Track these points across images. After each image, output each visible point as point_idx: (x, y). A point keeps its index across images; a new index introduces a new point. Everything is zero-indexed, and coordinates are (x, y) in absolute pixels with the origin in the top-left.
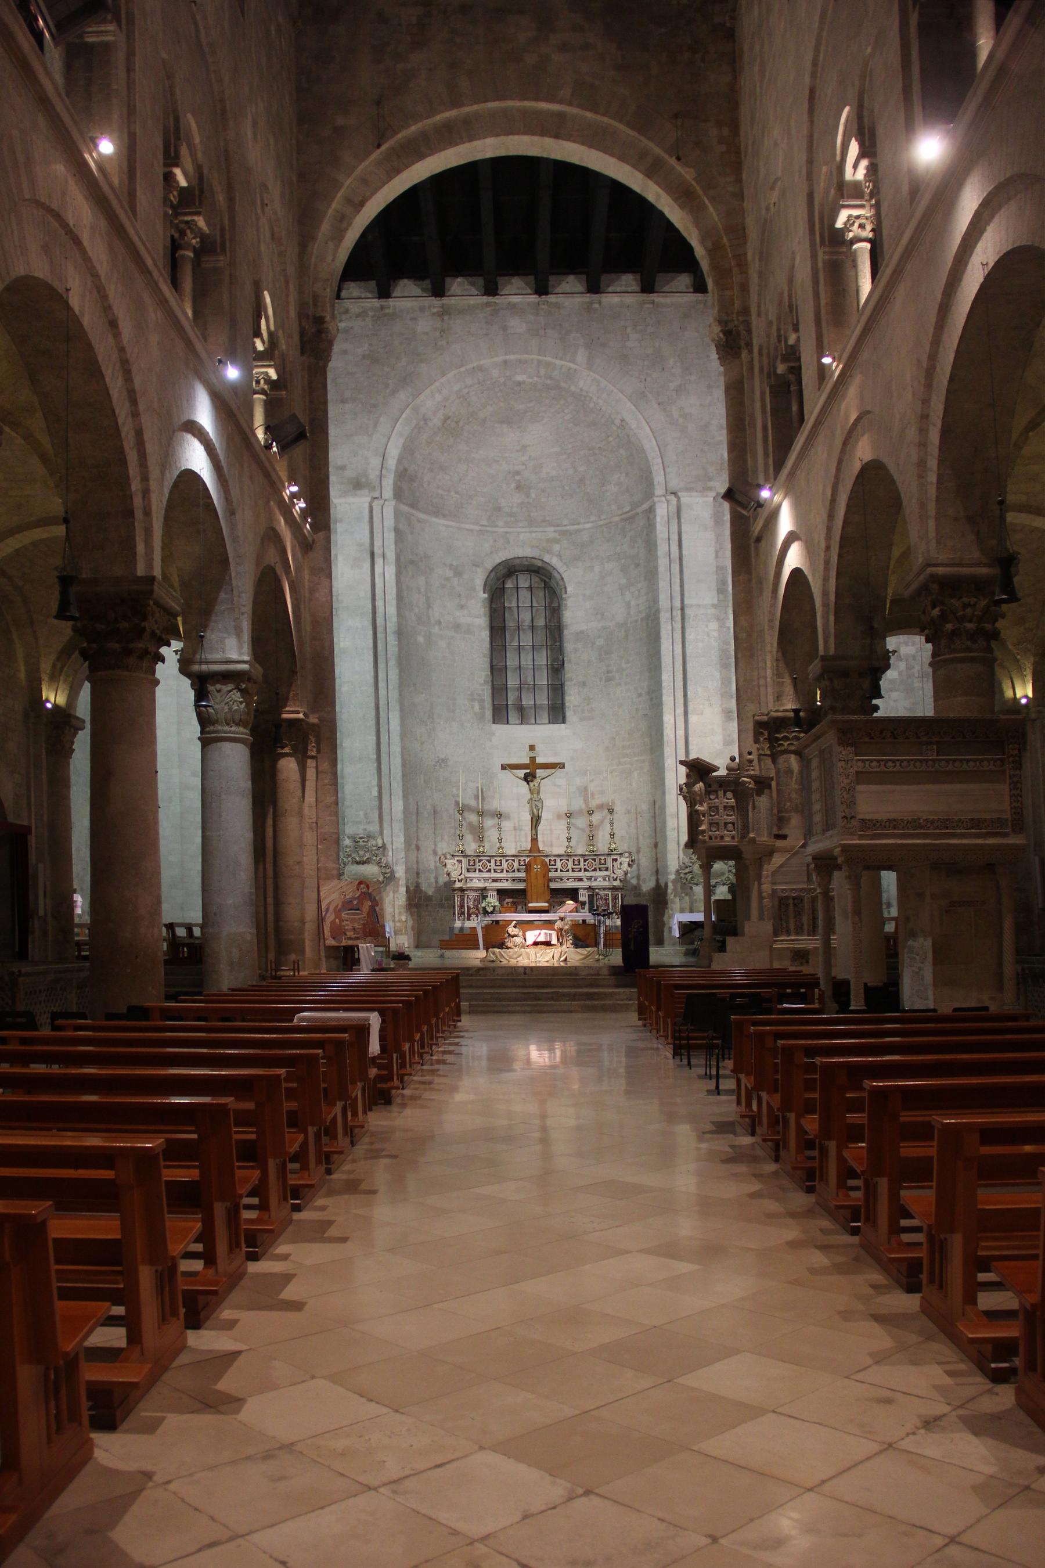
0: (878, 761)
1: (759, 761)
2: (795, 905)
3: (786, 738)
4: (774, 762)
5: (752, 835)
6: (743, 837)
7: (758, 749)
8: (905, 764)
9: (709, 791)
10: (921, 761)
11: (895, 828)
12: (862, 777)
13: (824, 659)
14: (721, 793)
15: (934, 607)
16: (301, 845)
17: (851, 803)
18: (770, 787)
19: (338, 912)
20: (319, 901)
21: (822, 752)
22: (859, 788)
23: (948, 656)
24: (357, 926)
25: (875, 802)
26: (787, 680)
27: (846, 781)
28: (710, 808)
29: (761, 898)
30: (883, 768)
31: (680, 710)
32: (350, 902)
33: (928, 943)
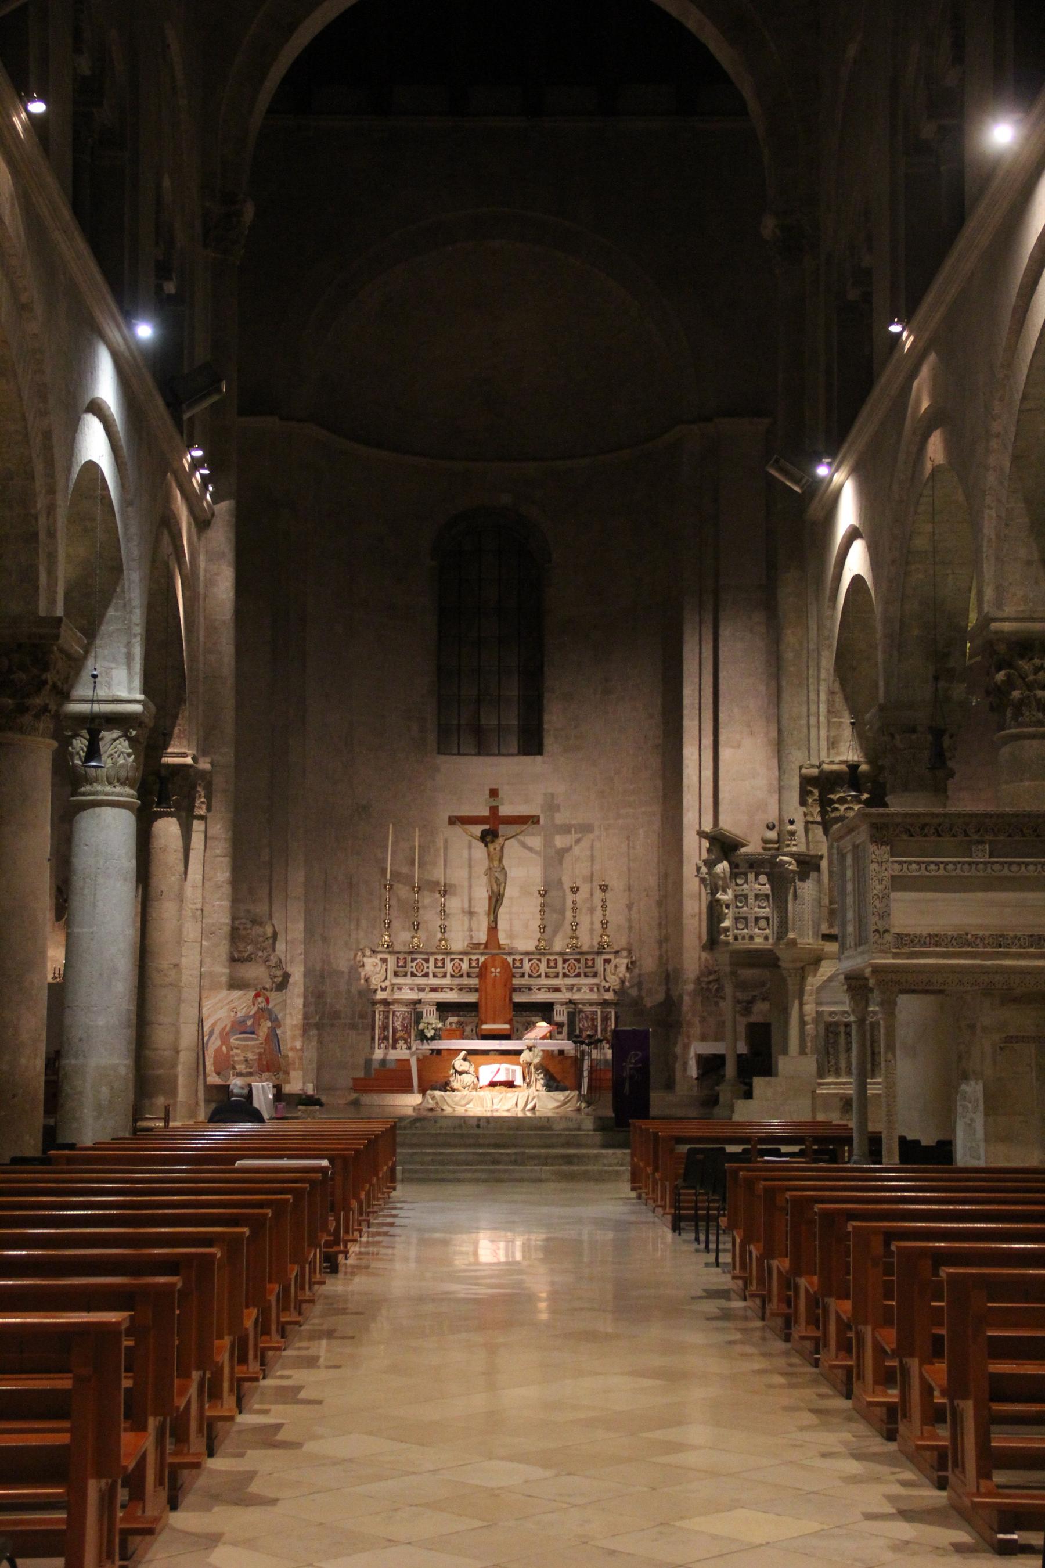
0: (918, 863)
1: (807, 831)
3: (842, 801)
4: (826, 832)
5: (791, 935)
7: (805, 815)
8: (950, 867)
9: (736, 872)
10: (970, 864)
11: (937, 946)
12: (899, 883)
13: (882, 708)
14: (751, 877)
15: (999, 669)
16: (180, 942)
17: (885, 915)
18: (818, 869)
19: (225, 1038)
20: (201, 1022)
21: (856, 847)
22: (895, 895)
23: (1014, 731)
24: (251, 1056)
25: (913, 913)
26: (847, 720)
27: (879, 887)
28: (736, 896)
29: (803, 1023)
30: (924, 872)
31: (708, 741)
32: (243, 1022)
33: (980, 1087)
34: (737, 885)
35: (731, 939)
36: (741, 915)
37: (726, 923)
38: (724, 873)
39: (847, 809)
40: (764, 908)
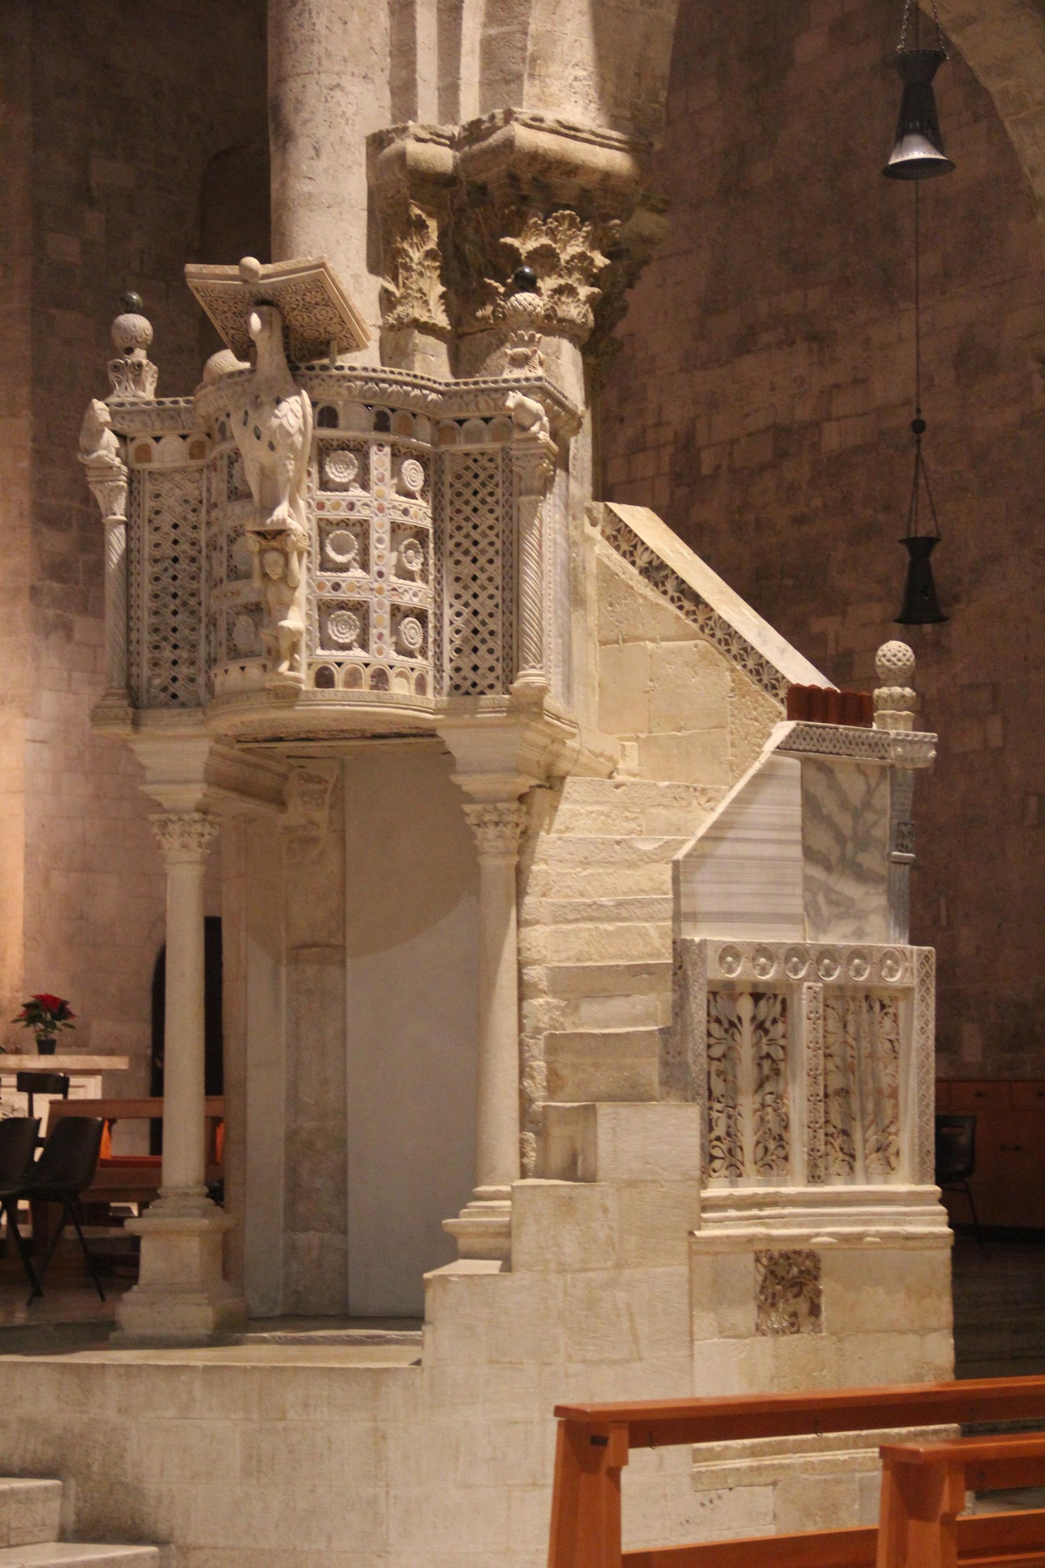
2: (760, 1027)
5: (530, 676)
6: (465, 690)
14: (380, 460)
28: (324, 528)
34: (325, 485)
35: (305, 677)
36: (341, 596)
37: (295, 620)
38: (302, 432)
39: (559, 291)
40: (410, 576)
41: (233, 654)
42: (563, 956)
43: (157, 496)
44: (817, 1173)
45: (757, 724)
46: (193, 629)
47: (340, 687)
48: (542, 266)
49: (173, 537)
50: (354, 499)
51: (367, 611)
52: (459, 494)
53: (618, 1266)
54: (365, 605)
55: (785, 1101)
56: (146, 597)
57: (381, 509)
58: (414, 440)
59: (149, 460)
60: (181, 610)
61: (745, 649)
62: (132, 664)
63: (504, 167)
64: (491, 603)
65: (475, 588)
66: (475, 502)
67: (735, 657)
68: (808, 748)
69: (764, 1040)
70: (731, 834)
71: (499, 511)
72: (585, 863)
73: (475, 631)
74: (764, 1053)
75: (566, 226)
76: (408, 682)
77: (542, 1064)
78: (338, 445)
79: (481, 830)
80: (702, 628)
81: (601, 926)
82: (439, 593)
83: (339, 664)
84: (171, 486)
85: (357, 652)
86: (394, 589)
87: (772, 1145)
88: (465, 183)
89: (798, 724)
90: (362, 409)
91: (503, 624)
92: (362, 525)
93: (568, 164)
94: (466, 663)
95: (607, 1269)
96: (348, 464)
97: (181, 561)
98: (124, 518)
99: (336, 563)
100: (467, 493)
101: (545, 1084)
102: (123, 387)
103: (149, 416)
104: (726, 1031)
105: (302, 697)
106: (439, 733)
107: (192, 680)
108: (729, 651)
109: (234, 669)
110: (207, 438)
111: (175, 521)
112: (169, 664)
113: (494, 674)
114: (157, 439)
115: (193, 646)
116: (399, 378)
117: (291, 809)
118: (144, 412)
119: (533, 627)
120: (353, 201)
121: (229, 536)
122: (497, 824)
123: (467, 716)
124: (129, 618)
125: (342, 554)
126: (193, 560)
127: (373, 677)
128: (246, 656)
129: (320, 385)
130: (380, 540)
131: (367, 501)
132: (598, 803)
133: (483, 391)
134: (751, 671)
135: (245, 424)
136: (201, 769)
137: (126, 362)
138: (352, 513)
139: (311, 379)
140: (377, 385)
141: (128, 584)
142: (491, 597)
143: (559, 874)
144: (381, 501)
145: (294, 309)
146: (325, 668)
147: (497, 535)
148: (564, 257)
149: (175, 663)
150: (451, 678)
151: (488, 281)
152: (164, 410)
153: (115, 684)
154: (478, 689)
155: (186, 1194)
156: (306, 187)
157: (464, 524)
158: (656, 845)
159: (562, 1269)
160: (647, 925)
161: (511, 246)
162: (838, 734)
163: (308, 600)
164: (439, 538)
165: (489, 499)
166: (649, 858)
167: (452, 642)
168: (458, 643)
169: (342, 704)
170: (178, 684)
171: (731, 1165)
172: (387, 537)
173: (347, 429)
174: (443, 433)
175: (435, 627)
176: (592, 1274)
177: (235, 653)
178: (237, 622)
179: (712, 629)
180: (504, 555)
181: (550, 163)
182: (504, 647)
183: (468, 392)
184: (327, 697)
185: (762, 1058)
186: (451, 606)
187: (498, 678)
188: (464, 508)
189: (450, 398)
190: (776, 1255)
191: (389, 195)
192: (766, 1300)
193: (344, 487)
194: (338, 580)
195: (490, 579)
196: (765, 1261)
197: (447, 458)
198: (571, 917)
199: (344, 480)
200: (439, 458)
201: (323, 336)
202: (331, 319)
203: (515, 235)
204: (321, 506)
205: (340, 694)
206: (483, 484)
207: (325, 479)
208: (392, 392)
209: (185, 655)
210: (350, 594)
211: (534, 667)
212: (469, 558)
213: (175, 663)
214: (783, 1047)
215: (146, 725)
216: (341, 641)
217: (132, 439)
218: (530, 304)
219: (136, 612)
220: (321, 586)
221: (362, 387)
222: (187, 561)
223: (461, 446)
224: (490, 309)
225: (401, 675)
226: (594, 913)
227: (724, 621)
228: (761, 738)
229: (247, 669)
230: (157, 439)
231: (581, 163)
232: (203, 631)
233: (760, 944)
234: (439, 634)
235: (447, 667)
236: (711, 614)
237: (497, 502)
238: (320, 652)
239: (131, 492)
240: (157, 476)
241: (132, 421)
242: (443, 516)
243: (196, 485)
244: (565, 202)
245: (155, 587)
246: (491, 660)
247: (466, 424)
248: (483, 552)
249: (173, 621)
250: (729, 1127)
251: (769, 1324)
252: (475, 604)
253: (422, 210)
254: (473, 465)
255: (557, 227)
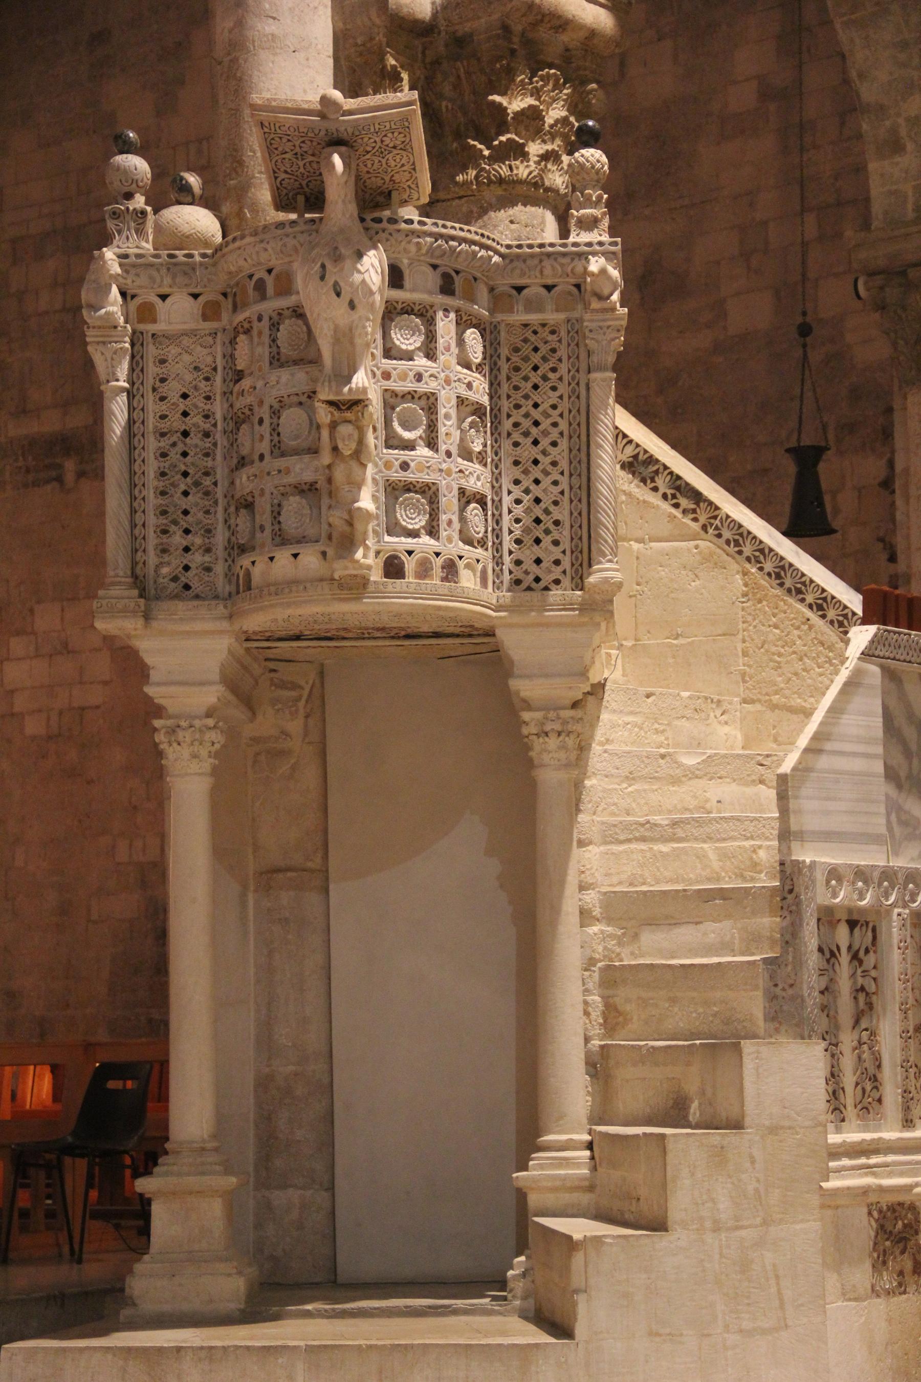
6: (528, 584)
14: (445, 326)
28: (391, 399)
34: (389, 352)
39: (545, 157)
41: (278, 539)
42: (615, 880)
43: (163, 362)
44: (910, 1117)
45: (777, 631)
46: (207, 512)
47: (410, 578)
48: (527, 129)
49: (182, 407)
50: (421, 369)
51: (436, 493)
52: (517, 369)
53: (765, 1223)
54: (434, 488)
55: (878, 1038)
56: (152, 475)
57: (448, 381)
58: (476, 307)
59: (154, 321)
60: (193, 490)
61: (762, 551)
62: (137, 551)
63: (496, 16)
64: (555, 490)
65: (536, 473)
66: (535, 378)
67: (748, 559)
68: (887, 654)
69: (859, 971)
70: (828, 746)
71: (563, 389)
72: (630, 778)
73: (538, 521)
74: (859, 987)
75: (550, 87)
76: (475, 575)
77: (597, 998)
78: (402, 309)
79: (541, 740)
80: (704, 528)
81: (655, 848)
82: (497, 478)
83: (410, 553)
84: (180, 350)
85: (425, 539)
86: (461, 471)
87: (868, 1086)
88: (443, 34)
89: (878, 629)
90: (429, 270)
91: (571, 513)
92: (428, 398)
93: (560, 17)
94: (528, 554)
95: (756, 1227)
96: (414, 331)
97: (192, 435)
98: (126, 385)
99: (401, 439)
100: (526, 369)
101: (601, 1021)
102: (124, 236)
103: (158, 270)
104: (828, 961)
105: (371, 588)
106: (498, 632)
107: (208, 569)
108: (740, 553)
109: (283, 557)
110: (221, 298)
111: (184, 390)
112: (180, 551)
113: (559, 569)
114: (164, 297)
115: (209, 531)
116: (468, 236)
117: (260, 718)
118: (152, 265)
119: (610, 517)
120: (320, 46)
121: (271, 407)
122: (559, 734)
123: (533, 614)
124: (133, 498)
125: (410, 431)
126: (207, 435)
127: (443, 568)
128: (299, 542)
129: (387, 240)
130: (447, 416)
131: (434, 371)
132: (632, 713)
133: (549, 255)
134: (769, 574)
135: (322, 278)
136: (218, 670)
137: (128, 209)
138: (420, 384)
139: (377, 233)
140: (447, 243)
141: (132, 461)
142: (555, 483)
143: (605, 790)
144: (447, 372)
145: (368, 152)
146: (395, 557)
147: (561, 415)
148: (549, 121)
149: (187, 549)
150: (511, 572)
151: (472, 142)
152: (175, 264)
153: (121, 573)
154: (542, 584)
155: (203, 1149)
156: (270, 27)
157: (522, 402)
158: (699, 760)
159: (716, 1229)
160: (705, 846)
161: (500, 104)
162: (911, 641)
163: (374, 479)
164: (496, 416)
165: (551, 375)
166: (693, 773)
167: (511, 532)
168: (517, 533)
169: (409, 598)
170: (190, 574)
171: (835, 1109)
172: (453, 413)
173: (413, 290)
174: (498, 301)
175: (493, 515)
176: (743, 1233)
177: (282, 539)
178: (284, 503)
179: (717, 528)
180: (570, 437)
181: (543, 16)
182: (572, 539)
183: (532, 256)
184: (398, 590)
185: (857, 991)
186: (509, 492)
187: (564, 572)
188: (522, 384)
189: (512, 261)
190: (885, 1208)
191: (359, 42)
192: (878, 1257)
193: (409, 356)
194: (406, 458)
195: (554, 464)
196: (875, 1214)
197: (502, 327)
198: (622, 838)
199: (411, 348)
200: (495, 327)
201: (386, 186)
202: (403, 165)
203: (503, 94)
204: (387, 376)
205: (413, 586)
206: (544, 359)
207: (389, 345)
208: (460, 252)
209: (198, 541)
210: (419, 475)
211: (610, 561)
212: (530, 440)
213: (187, 549)
214: (875, 979)
215: (156, 619)
216: (410, 527)
217: (133, 297)
218: (598, 161)
219: (140, 492)
220: (388, 465)
221: (432, 244)
222: (200, 435)
223: (520, 316)
224: (472, 173)
225: (468, 566)
226: (647, 833)
227: (733, 520)
228: (783, 647)
229: (300, 557)
230: (164, 297)
231: (570, 16)
232: (220, 516)
233: (858, 866)
234: (497, 523)
235: (507, 559)
236: (716, 513)
237: (561, 379)
238: (387, 538)
239: (133, 357)
240: (162, 339)
241: (137, 275)
242: (500, 392)
243: (209, 350)
244: (549, 60)
245: (162, 464)
246: (556, 553)
247: (525, 292)
248: (545, 433)
249: (184, 503)
250: (833, 1067)
251: (882, 1284)
252: (536, 491)
253: (396, 61)
254: (533, 338)
255: (543, 86)
